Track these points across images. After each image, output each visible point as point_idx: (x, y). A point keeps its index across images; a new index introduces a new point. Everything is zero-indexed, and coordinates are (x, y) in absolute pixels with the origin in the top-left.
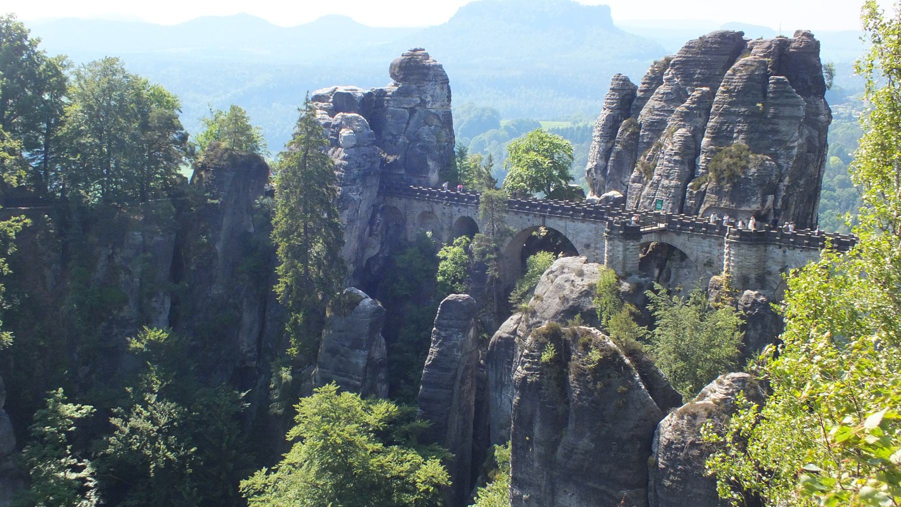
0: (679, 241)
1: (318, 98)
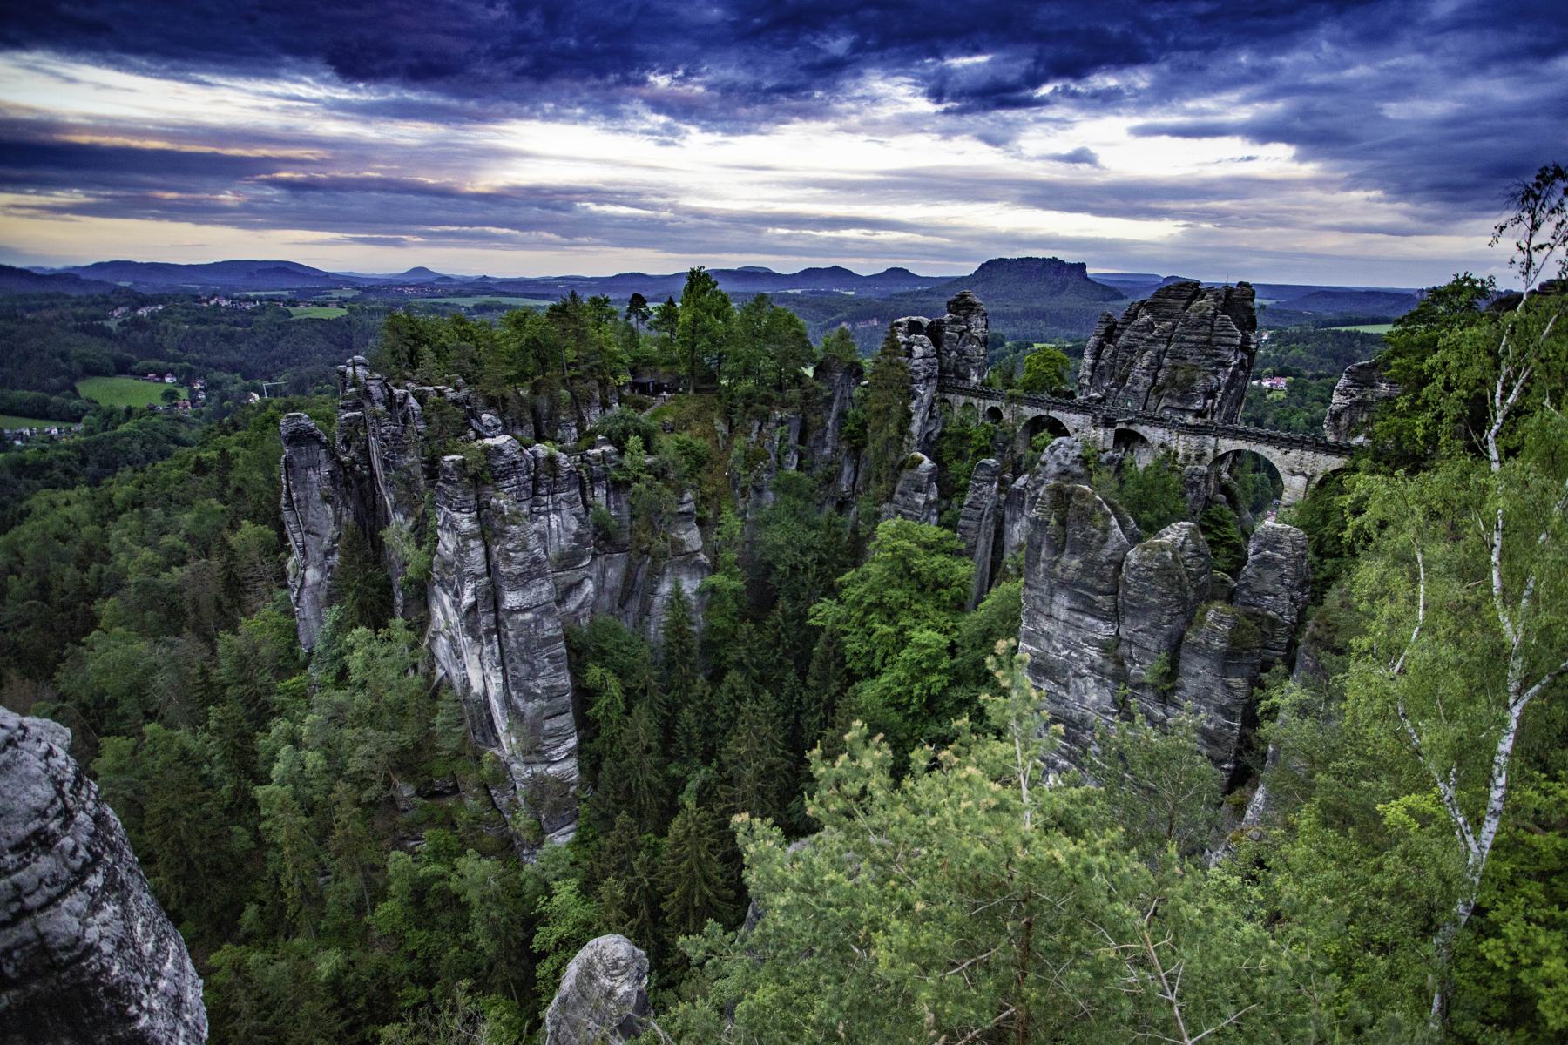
0: (1141, 429)
1: (899, 325)
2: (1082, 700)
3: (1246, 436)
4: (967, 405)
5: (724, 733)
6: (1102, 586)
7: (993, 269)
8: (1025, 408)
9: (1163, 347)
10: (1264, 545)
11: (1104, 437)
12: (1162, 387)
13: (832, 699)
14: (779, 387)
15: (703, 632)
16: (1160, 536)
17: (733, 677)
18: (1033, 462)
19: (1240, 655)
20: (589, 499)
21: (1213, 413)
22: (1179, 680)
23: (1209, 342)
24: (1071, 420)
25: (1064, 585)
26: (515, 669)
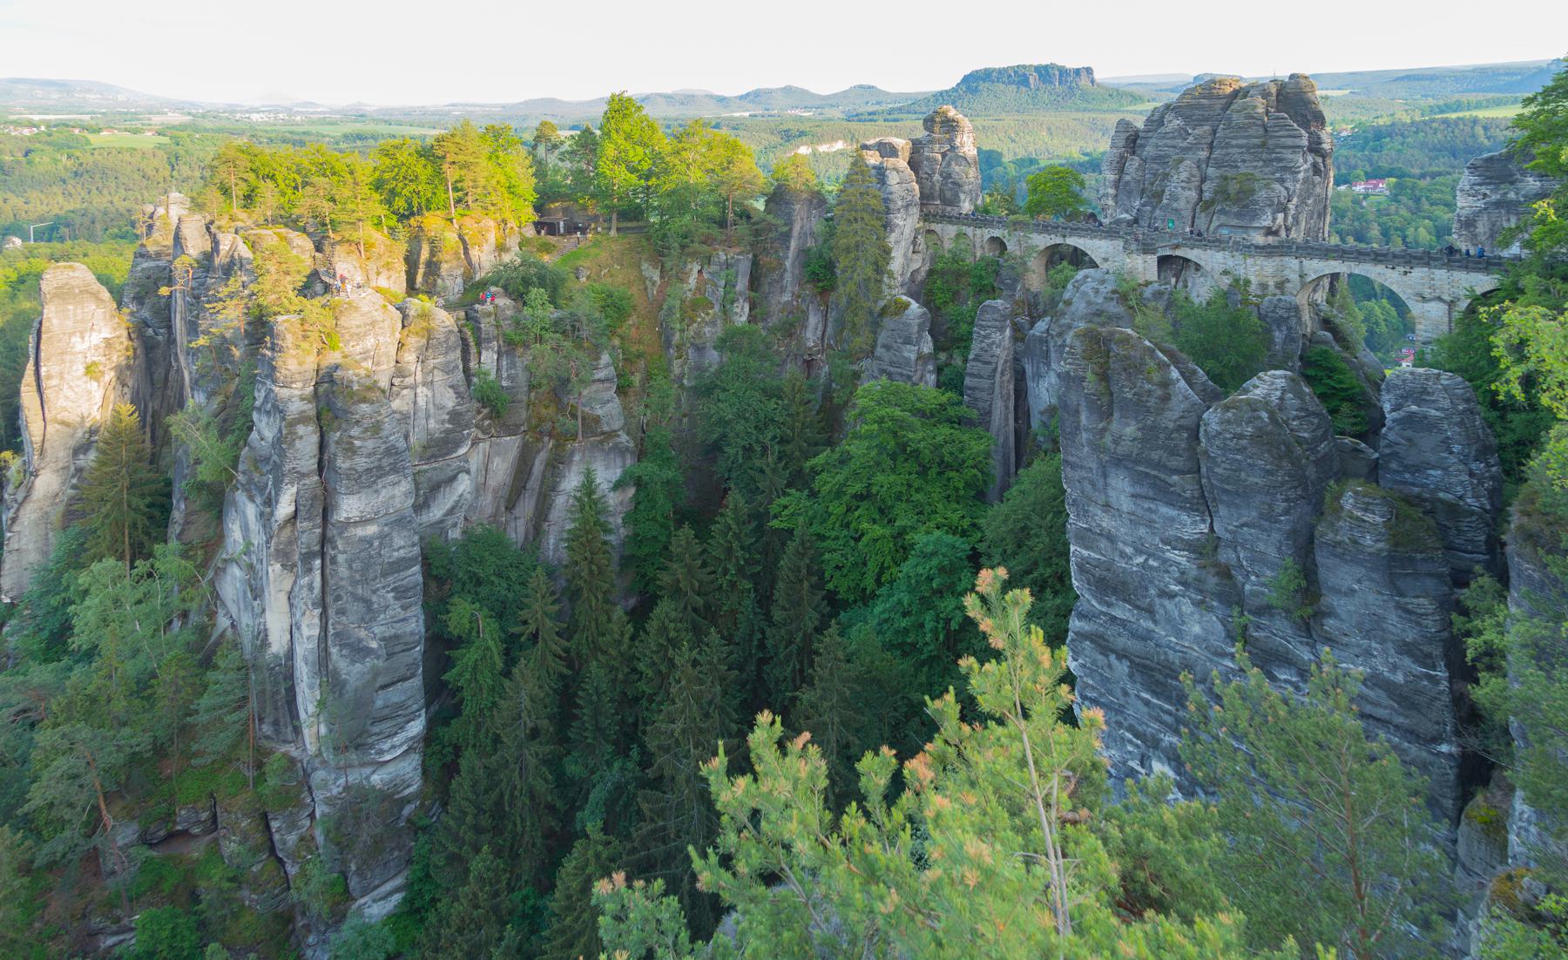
0: (1192, 254)
1: (865, 147)
2: (1179, 634)
3: (1341, 254)
4: (959, 235)
5: (651, 701)
6: (1175, 462)
7: (975, 82)
8: (1034, 236)
9: (1203, 154)
10: (1405, 398)
11: (1144, 267)
12: (1208, 205)
13: (807, 639)
14: (722, 223)
15: (623, 544)
16: (1246, 391)
17: (664, 609)
18: (1053, 303)
19: (1412, 560)
20: (473, 365)
21: (1288, 229)
22: (1323, 600)
23: (1264, 145)
24: (1095, 247)
25: (1119, 462)
26: (341, 612)
